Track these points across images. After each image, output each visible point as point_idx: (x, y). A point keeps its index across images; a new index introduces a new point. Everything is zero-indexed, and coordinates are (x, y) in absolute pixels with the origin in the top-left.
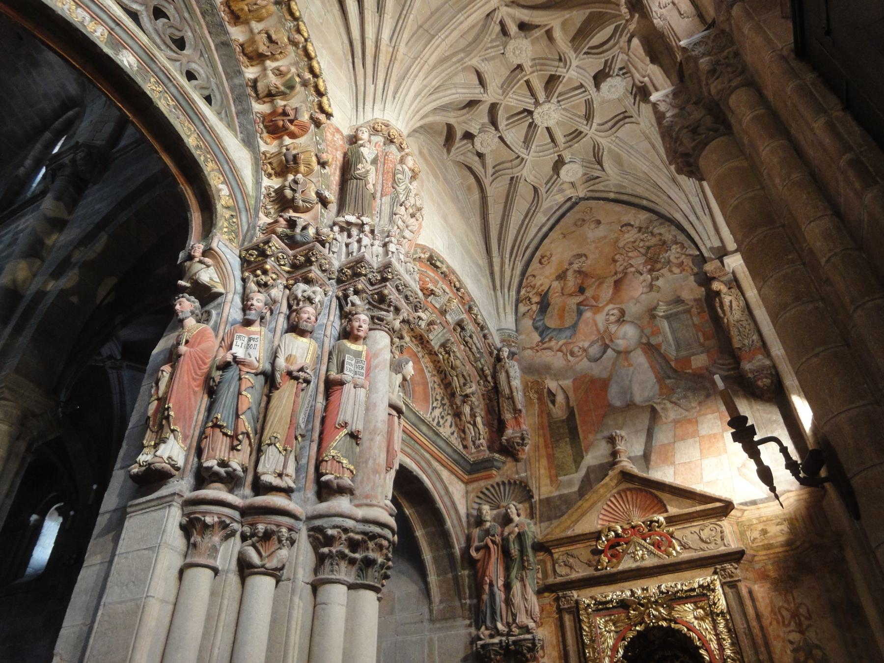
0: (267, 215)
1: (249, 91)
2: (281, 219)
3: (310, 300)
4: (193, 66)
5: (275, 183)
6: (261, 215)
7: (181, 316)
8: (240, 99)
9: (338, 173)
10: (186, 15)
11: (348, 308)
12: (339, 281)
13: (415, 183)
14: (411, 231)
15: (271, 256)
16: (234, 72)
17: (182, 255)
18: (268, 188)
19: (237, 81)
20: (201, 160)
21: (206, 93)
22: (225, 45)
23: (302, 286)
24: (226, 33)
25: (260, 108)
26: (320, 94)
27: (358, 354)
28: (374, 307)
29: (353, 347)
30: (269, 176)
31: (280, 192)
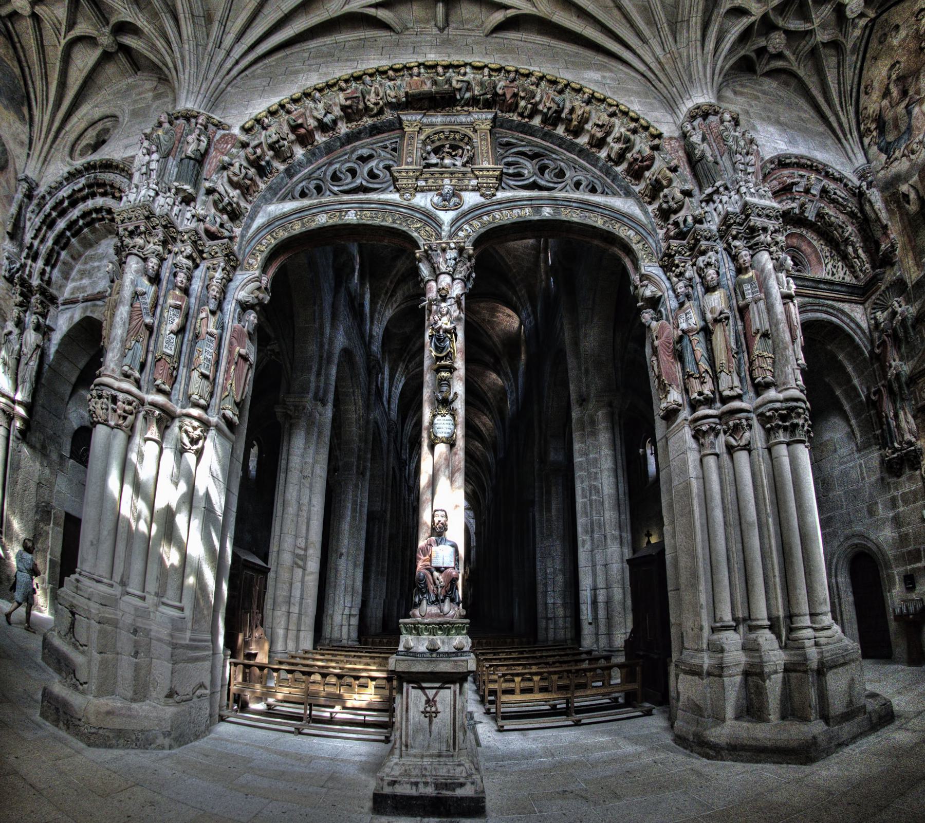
0: (662, 228)
1: (610, 164)
2: (669, 226)
3: (709, 264)
4: (575, 179)
5: (656, 205)
6: (659, 231)
7: (647, 324)
8: (608, 172)
9: (687, 166)
10: (554, 156)
11: (733, 253)
12: (721, 237)
13: (738, 129)
14: (752, 165)
15: (675, 255)
16: (594, 161)
17: (632, 288)
18: (653, 211)
19: (600, 165)
20: (611, 229)
21: (590, 186)
22: (581, 152)
23: (701, 259)
24: (577, 144)
25: (619, 169)
26: (646, 128)
27: (750, 280)
28: (749, 238)
29: (746, 276)
30: (650, 203)
31: (660, 209)
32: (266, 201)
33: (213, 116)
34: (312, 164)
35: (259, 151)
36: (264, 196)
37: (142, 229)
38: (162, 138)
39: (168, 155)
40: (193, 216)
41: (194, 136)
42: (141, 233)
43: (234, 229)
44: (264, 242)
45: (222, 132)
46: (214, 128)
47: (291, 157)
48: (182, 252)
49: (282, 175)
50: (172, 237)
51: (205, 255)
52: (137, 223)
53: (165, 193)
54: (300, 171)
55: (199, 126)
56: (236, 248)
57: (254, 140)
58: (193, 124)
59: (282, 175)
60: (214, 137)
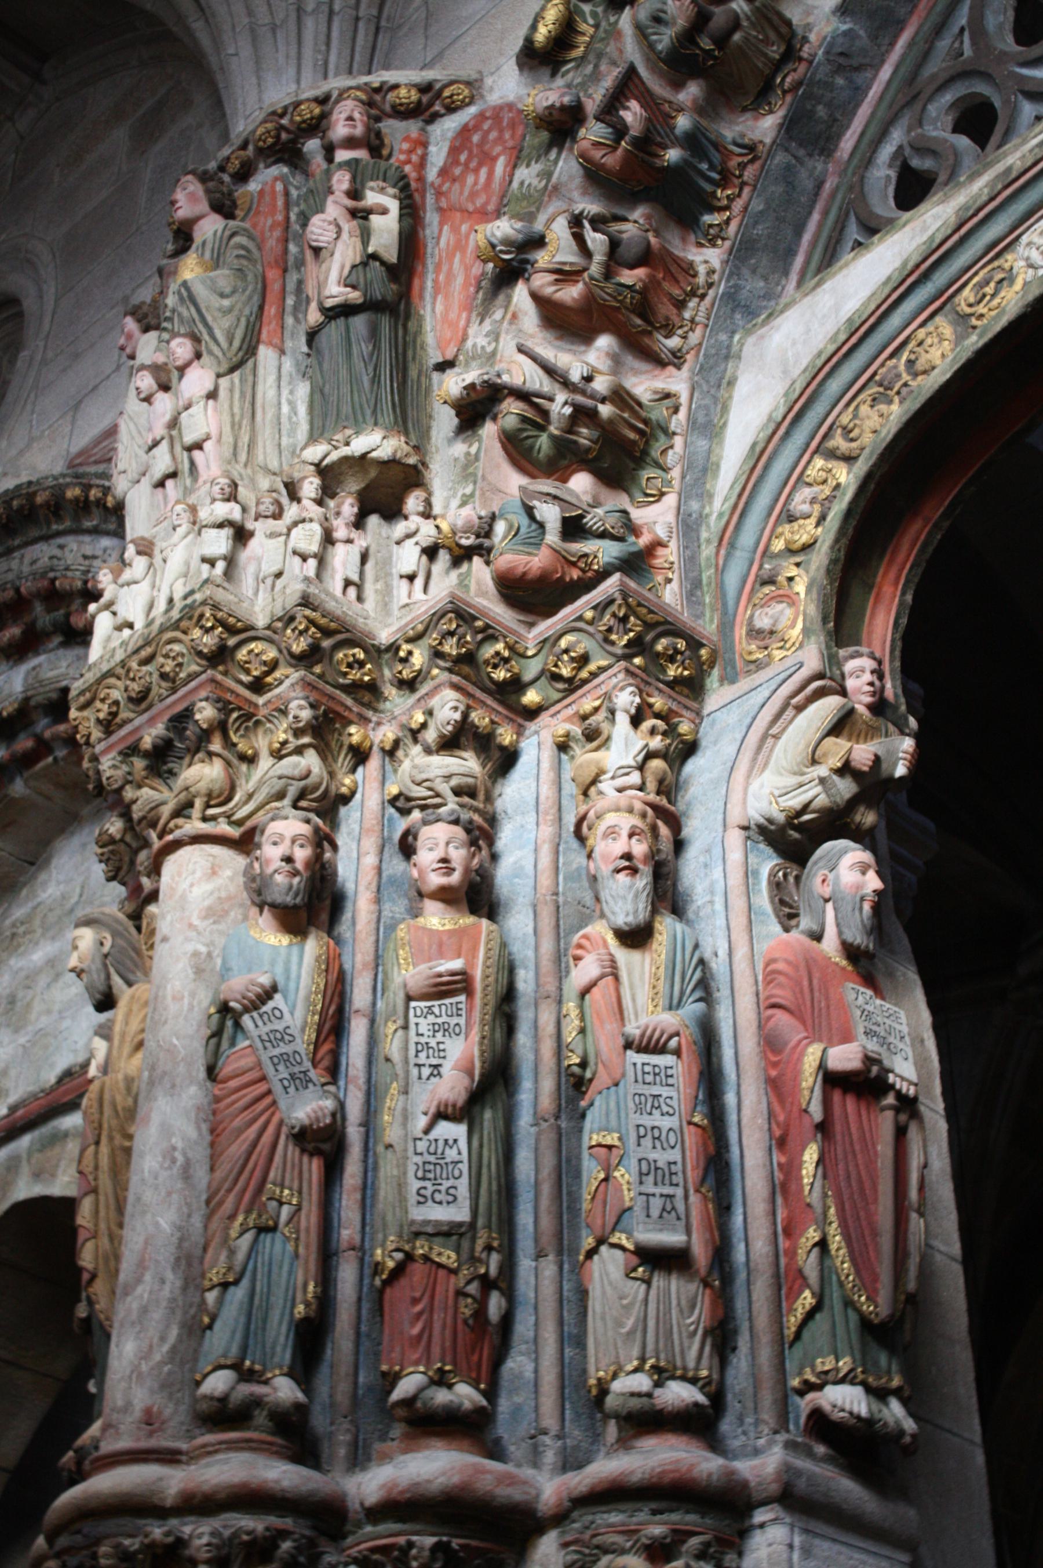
32: (751, 313)
33: (390, 76)
34: (900, 25)
35: (632, 114)
36: (731, 298)
37: (206, 713)
38: (201, 291)
39: (250, 350)
40: (431, 552)
41: (335, 208)
42: (205, 735)
43: (638, 515)
44: (801, 501)
45: (451, 124)
46: (412, 127)
47: (790, 54)
48: (415, 734)
49: (780, 158)
50: (354, 689)
51: (531, 697)
52: (174, 704)
53: (278, 515)
54: (858, 93)
55: (342, 155)
56: (671, 595)
57: (596, 77)
58: (318, 162)
59: (780, 158)
60: (422, 164)
